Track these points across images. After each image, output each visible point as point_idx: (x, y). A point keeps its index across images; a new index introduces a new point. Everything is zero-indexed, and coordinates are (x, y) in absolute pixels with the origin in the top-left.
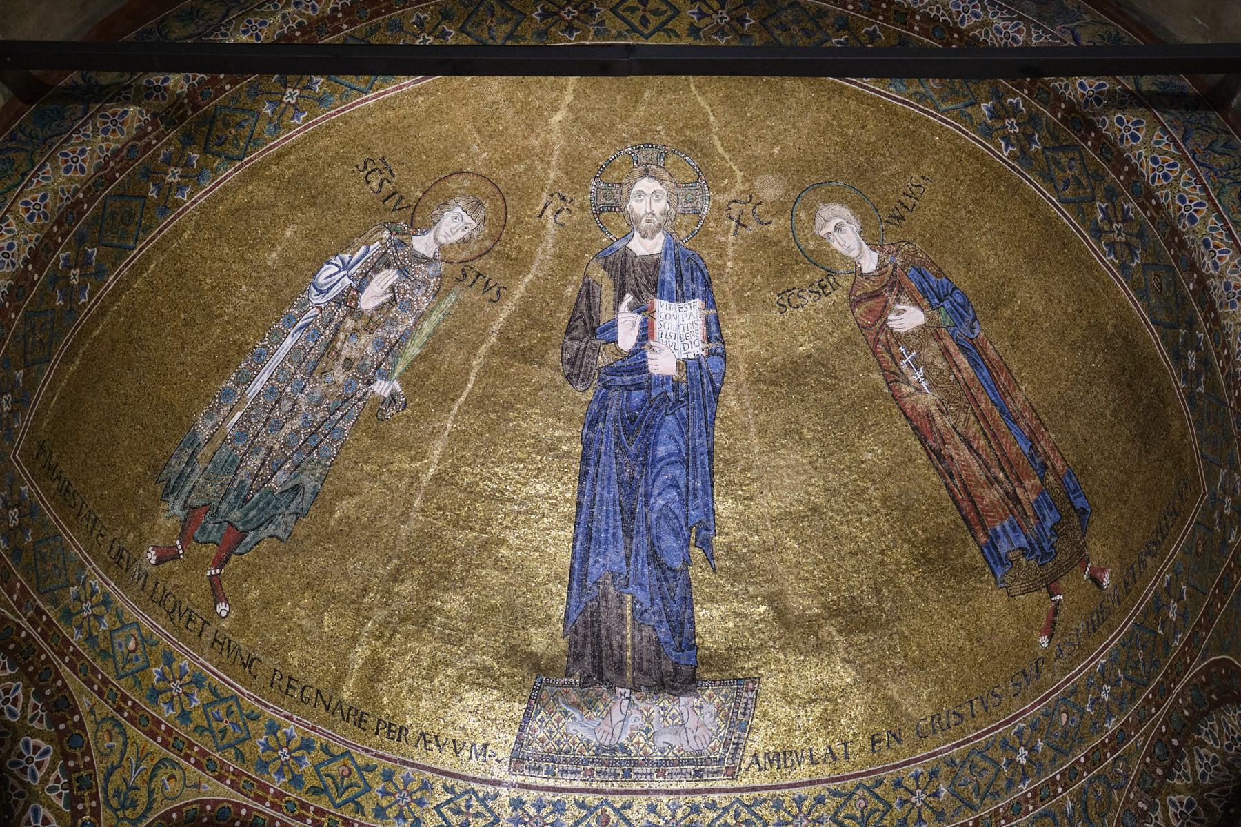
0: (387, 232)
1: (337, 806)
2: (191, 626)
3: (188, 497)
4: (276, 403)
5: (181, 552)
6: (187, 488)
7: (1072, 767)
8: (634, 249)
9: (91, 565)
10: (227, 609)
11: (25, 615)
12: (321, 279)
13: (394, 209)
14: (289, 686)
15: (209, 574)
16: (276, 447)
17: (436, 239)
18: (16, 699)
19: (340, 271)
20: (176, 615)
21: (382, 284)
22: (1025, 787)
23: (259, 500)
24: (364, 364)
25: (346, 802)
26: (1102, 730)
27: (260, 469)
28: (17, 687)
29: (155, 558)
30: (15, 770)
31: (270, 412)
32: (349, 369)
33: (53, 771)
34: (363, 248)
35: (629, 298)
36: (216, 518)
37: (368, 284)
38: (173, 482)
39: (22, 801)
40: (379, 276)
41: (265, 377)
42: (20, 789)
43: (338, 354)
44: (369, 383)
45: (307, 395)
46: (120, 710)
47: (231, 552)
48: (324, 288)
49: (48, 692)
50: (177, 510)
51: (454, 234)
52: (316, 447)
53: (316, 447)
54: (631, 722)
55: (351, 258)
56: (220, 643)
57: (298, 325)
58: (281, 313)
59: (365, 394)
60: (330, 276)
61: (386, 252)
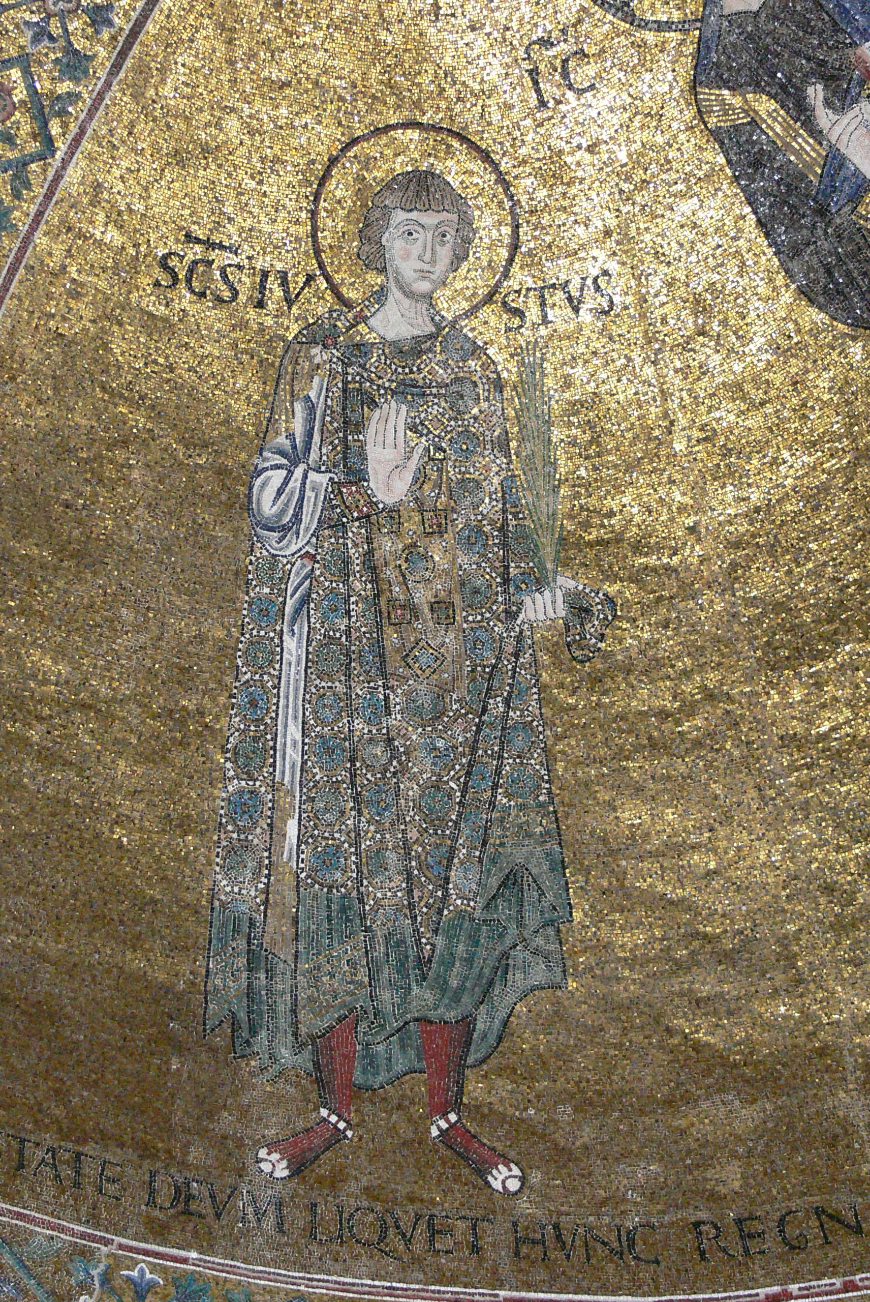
0: (316, 350)
3: (295, 1024)
4: (352, 761)
5: (342, 1125)
6: (283, 1007)
8: (741, 7)
9: (107, 1242)
10: (516, 1171)
12: (267, 506)
13: (290, 302)
15: (435, 1132)
16: (413, 834)
17: (409, 294)
19: (290, 473)
20: (395, 1240)
21: (390, 440)
23: (449, 947)
24: (476, 591)
27: (410, 892)
29: (284, 1163)
31: (353, 784)
32: (451, 620)
34: (298, 407)
35: (816, 93)
36: (383, 1027)
37: (363, 458)
38: (242, 1015)
40: (371, 431)
41: (294, 732)
43: (414, 610)
44: (511, 616)
45: (402, 712)
47: (461, 1067)
48: (286, 520)
50: (285, 1053)
51: (433, 262)
52: (495, 786)
53: (495, 786)
55: (291, 436)
56: (534, 1242)
57: (288, 610)
58: (239, 611)
59: (520, 638)
60: (280, 492)
61: (345, 383)
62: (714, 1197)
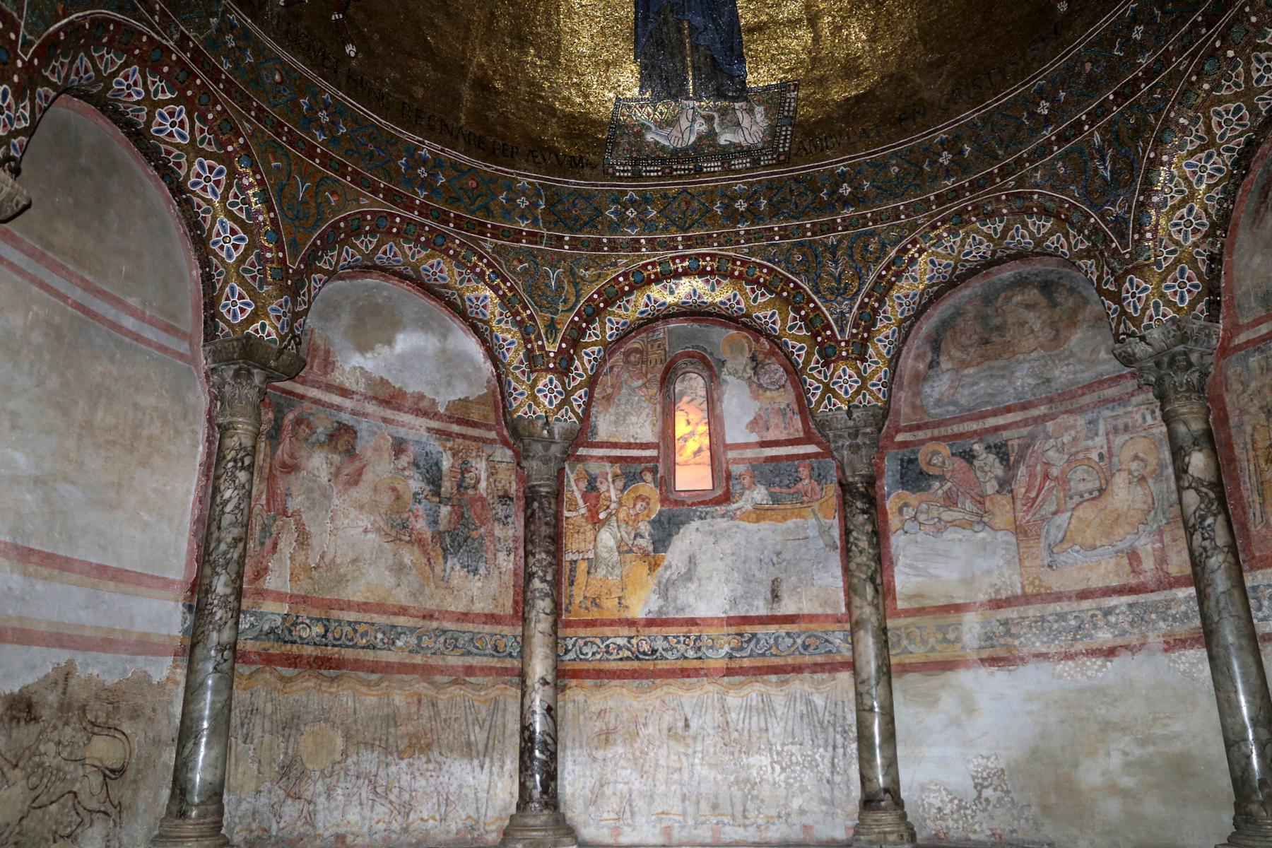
1: (472, 213)
2: (327, 63)
7: (1101, 105)
11: (171, 38)
14: (418, 116)
18: (182, 122)
22: (1049, 133)
25: (479, 209)
26: (1135, 66)
28: (181, 111)
30: (197, 189)
33: (231, 187)
39: (209, 216)
42: (205, 206)
46: (279, 135)
49: (210, 116)
54: (696, 127)
62: (412, 96)
